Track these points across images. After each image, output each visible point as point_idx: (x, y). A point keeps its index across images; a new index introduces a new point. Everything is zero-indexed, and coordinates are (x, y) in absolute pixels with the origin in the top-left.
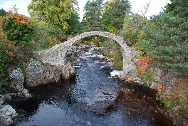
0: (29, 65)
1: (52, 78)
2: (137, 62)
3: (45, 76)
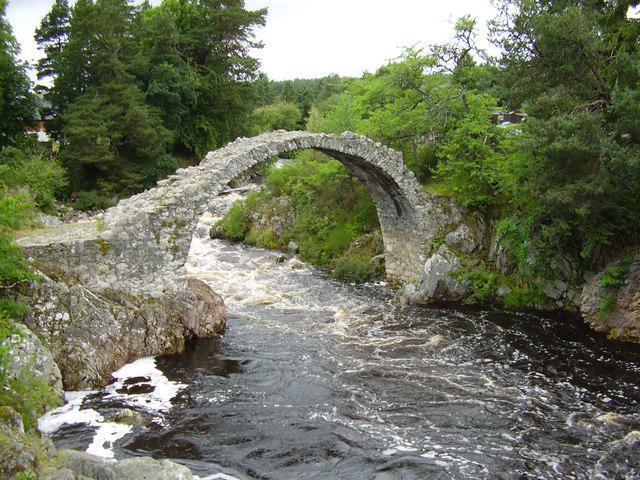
0: (49, 305)
2: (459, 245)
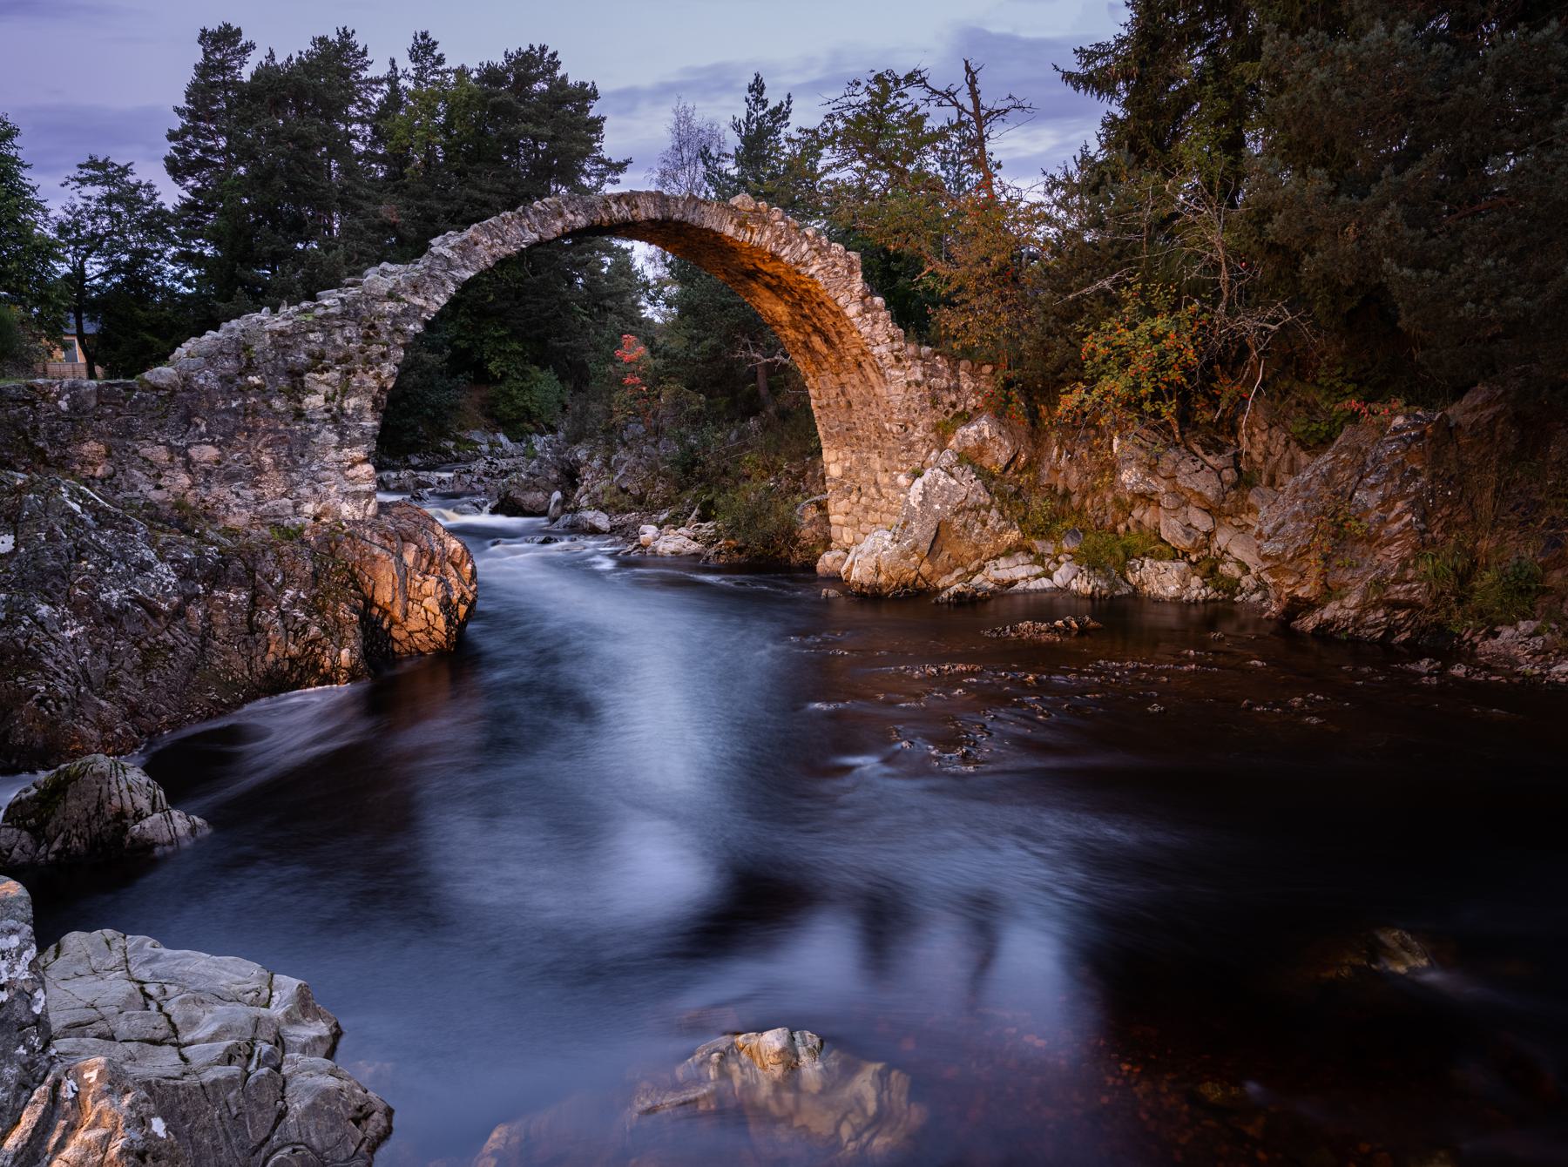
1: (294, 650)
3: (206, 636)
